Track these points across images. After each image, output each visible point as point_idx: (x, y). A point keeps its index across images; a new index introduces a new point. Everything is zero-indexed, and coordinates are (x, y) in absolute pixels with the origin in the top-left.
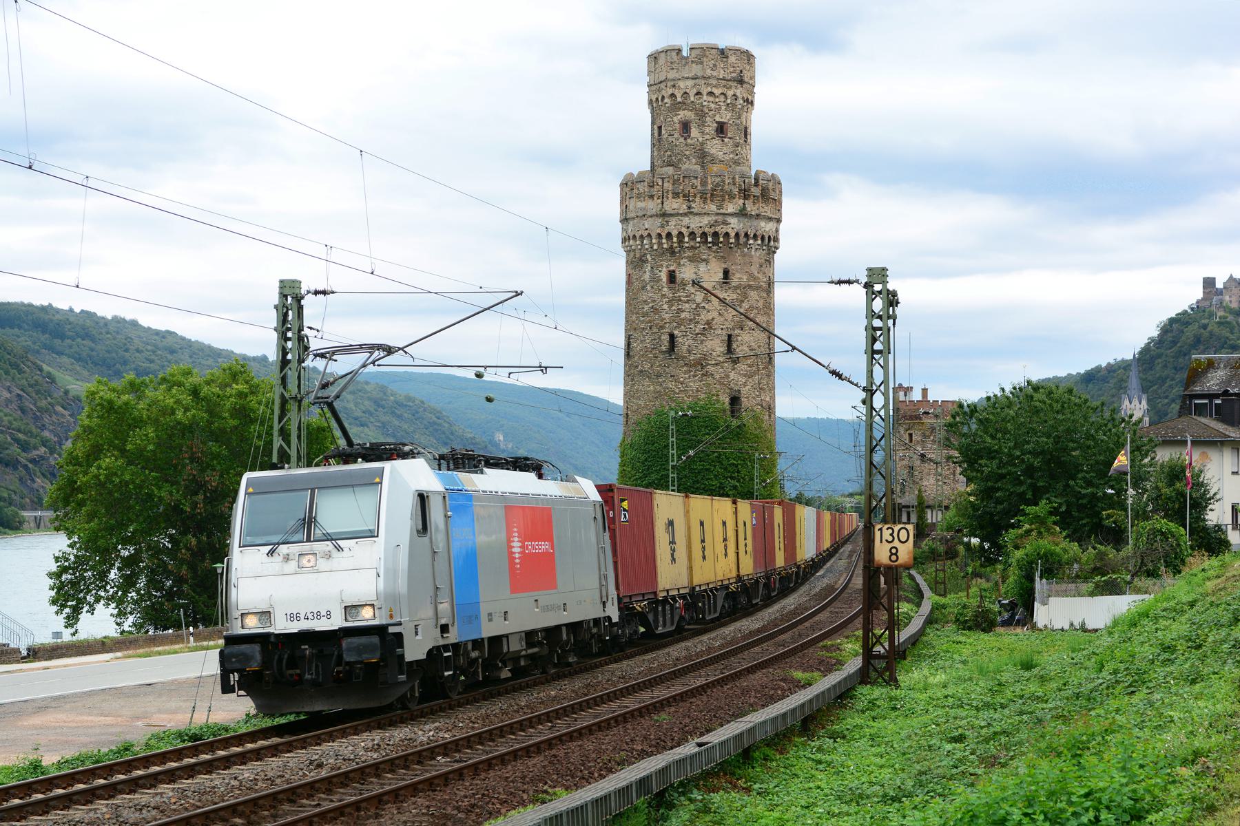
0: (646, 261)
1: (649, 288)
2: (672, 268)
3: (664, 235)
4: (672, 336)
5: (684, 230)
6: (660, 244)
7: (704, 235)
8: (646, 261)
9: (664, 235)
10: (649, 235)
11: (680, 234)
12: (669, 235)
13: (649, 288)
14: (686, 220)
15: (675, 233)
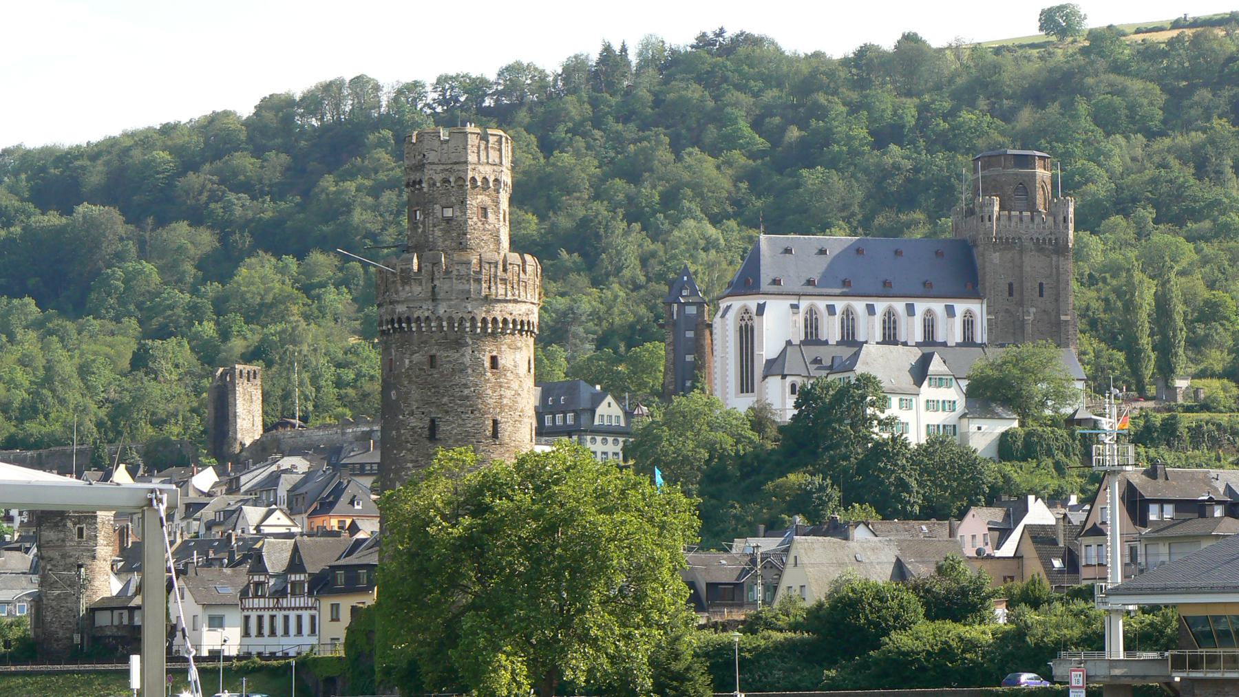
0: (466, 345)
1: (470, 371)
2: (494, 354)
3: (489, 319)
4: (495, 422)
5: (510, 318)
6: (484, 328)
7: (522, 323)
8: (466, 345)
9: (489, 319)
10: (473, 319)
11: (505, 321)
12: (495, 320)
13: (470, 371)
14: (510, 306)
15: (500, 319)
